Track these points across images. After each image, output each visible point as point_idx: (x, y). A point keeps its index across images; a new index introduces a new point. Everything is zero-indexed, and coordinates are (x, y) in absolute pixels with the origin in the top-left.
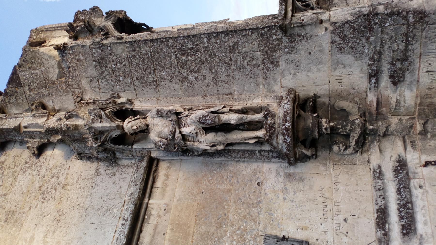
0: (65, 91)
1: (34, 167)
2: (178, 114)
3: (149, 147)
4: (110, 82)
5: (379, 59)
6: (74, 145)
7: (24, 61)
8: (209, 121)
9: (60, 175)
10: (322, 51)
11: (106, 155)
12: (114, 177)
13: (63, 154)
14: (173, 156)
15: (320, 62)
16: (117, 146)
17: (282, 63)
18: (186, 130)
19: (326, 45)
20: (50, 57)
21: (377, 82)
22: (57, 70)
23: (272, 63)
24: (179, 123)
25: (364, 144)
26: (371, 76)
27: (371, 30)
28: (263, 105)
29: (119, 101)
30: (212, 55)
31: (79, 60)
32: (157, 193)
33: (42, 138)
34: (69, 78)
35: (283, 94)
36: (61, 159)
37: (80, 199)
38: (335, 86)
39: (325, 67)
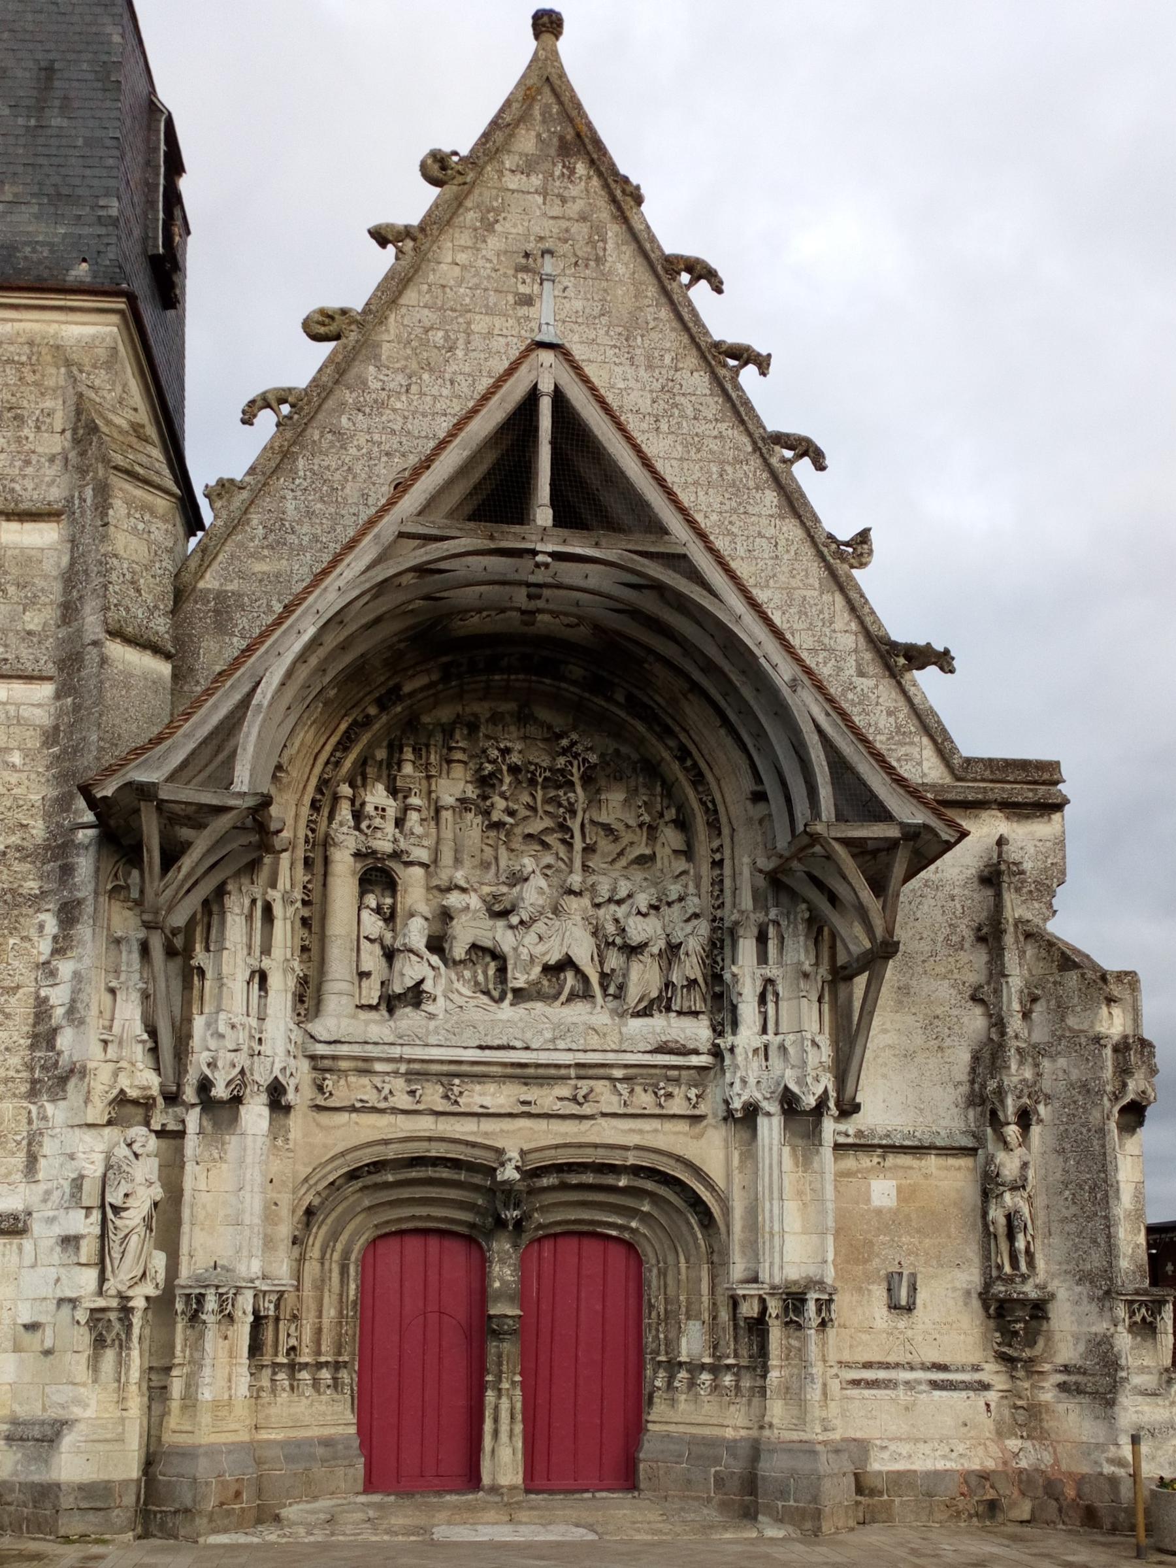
0: (1053, 1034)
2: (1024, 1187)
4: (1063, 1095)
5: (1079, 1373)
8: (1016, 1223)
10: (1089, 1325)
15: (1080, 1323)
17: (1079, 1289)
18: (1007, 1197)
19: (1094, 1329)
20: (1092, 1022)
21: (1061, 1371)
22: (1076, 1027)
23: (1080, 1279)
24: (1014, 1189)
25: (1003, 1359)
26: (1065, 1366)
27: (1105, 1366)
28: (1037, 1270)
29: (1041, 1108)
30: (1089, 1219)
31: (1087, 1059)
35: (1049, 1289)
38: (1057, 1336)
39: (1075, 1328)
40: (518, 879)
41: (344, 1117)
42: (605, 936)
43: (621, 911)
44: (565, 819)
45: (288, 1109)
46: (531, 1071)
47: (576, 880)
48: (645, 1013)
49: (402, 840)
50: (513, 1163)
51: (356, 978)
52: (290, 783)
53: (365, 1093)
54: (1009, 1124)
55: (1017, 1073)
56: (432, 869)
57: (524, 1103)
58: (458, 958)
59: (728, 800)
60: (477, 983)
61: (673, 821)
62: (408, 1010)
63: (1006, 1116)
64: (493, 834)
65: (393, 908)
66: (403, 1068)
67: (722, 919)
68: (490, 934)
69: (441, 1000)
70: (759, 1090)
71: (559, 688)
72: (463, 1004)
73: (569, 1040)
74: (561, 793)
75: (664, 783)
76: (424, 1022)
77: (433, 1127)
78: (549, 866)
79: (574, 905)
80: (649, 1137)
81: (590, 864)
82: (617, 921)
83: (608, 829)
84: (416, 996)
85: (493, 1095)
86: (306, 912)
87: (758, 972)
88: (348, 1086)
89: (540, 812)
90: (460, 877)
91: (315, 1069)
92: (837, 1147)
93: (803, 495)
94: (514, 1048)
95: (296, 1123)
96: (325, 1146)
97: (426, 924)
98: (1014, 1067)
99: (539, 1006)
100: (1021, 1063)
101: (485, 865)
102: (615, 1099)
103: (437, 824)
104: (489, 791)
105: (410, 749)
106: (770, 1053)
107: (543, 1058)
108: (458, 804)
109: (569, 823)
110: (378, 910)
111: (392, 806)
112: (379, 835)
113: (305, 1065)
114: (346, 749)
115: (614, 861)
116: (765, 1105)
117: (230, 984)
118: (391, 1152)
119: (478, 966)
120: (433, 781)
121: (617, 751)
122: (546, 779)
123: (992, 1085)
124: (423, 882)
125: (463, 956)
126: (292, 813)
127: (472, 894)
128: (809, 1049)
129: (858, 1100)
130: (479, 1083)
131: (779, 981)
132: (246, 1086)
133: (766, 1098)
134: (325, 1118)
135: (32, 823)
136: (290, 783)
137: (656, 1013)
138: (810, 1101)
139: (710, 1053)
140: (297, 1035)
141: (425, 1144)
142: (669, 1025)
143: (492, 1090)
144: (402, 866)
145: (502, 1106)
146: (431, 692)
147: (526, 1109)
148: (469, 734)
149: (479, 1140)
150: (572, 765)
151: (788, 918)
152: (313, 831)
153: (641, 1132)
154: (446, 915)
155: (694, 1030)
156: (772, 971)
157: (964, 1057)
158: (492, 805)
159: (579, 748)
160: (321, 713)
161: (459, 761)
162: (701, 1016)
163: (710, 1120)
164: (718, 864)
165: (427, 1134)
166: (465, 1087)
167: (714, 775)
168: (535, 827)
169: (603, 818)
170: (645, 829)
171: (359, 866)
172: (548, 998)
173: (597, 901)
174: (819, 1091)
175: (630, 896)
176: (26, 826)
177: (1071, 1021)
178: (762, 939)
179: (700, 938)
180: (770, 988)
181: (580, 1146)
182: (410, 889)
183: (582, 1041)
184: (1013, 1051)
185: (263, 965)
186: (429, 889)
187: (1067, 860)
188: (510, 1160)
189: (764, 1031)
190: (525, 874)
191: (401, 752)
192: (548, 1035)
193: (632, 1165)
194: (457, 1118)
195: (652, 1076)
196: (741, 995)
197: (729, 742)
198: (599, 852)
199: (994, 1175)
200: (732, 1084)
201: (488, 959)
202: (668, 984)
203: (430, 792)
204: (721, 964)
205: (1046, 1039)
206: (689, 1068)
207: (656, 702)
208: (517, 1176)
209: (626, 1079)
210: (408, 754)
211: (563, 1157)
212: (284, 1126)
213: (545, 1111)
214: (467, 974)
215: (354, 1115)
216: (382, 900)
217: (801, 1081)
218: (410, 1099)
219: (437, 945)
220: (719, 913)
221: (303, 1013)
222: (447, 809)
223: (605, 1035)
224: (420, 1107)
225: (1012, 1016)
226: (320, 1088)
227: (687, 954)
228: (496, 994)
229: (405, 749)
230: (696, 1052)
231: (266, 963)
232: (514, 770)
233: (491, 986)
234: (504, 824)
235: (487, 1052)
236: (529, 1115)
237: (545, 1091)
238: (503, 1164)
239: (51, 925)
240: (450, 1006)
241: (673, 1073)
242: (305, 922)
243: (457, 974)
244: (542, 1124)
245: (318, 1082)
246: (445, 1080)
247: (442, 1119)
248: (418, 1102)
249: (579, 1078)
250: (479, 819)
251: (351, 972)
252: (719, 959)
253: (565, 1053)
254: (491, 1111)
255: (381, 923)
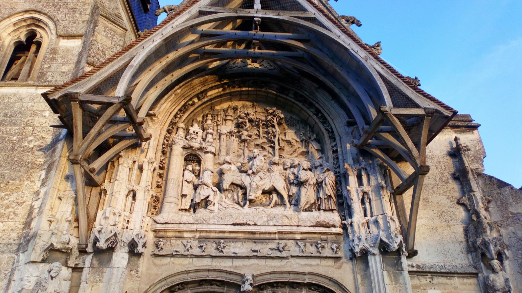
1: (452, 203)
3: (484, 272)
6: (472, 227)
7: (516, 191)
9: (453, 221)
11: (472, 247)
12: (460, 253)
13: (464, 218)
14: (482, 286)
16: (480, 255)
32: (461, 280)
33: (470, 206)
34: (512, 219)
36: (460, 218)
37: (445, 237)
40: (251, 159)
41: (167, 260)
42: (289, 180)
43: (295, 170)
44: (271, 138)
45: (139, 255)
46: (257, 236)
47: (276, 159)
48: (309, 210)
49: (204, 143)
50: (249, 282)
51: (180, 197)
52: (158, 122)
53: (179, 248)
54: (493, 259)
55: (491, 235)
56: (217, 156)
57: (254, 251)
58: (225, 188)
59: (337, 127)
60: (234, 199)
61: (315, 139)
62: (202, 210)
63: (491, 255)
64: (242, 145)
65: (199, 171)
66: (197, 235)
67: (339, 172)
68: (239, 178)
69: (217, 205)
70: (367, 243)
71: (268, 93)
72: (227, 206)
73: (275, 221)
74: (270, 129)
75: (310, 127)
76: (209, 214)
77: (210, 264)
78: (265, 156)
79: (275, 168)
80: (315, 268)
81: (282, 155)
82: (294, 174)
83: (289, 142)
84: (206, 202)
85: (240, 248)
86: (161, 172)
87: (359, 189)
88: (171, 244)
89: (261, 136)
90: (228, 159)
91: (156, 237)
92: (410, 272)
93: (354, 33)
94: (249, 225)
95: (144, 263)
96: (157, 275)
97: (212, 174)
98: (488, 232)
99: (261, 208)
100: (491, 230)
101: (239, 156)
102: (297, 249)
103: (220, 141)
104: (241, 129)
105: (211, 116)
106: (370, 225)
107: (263, 229)
108: (228, 134)
109: (273, 139)
110: (193, 172)
111: (200, 131)
112: (194, 140)
113: (151, 236)
114: (184, 113)
115: (291, 154)
116: (371, 249)
117: (117, 195)
118: (189, 278)
119: (234, 192)
120: (219, 127)
121: (291, 117)
122: (263, 124)
123: (479, 241)
124: (212, 160)
125: (227, 187)
126: (159, 133)
127: (233, 165)
128: (390, 221)
129: (415, 249)
130: (233, 242)
131: (370, 193)
132: (117, 243)
133: (371, 247)
134: (158, 261)
135: (47, 136)
136: (158, 122)
137: (314, 210)
138: (395, 246)
139: (340, 227)
140: (148, 221)
141: (206, 273)
142: (320, 214)
143: (239, 245)
144: (204, 154)
145: (244, 253)
146: (219, 94)
147: (255, 254)
148: (234, 112)
149: (232, 270)
150: (274, 119)
151: (370, 166)
152: (167, 141)
153: (311, 265)
154: (221, 173)
155: (332, 217)
156: (366, 187)
157: (459, 229)
158: (242, 134)
159: (276, 113)
160: (174, 98)
161: (229, 120)
162: (334, 211)
163: (344, 260)
164: (335, 152)
165: (207, 268)
166: (226, 244)
167: (331, 118)
168: (260, 141)
169: (287, 138)
170: (304, 142)
171: (185, 152)
172: (265, 205)
173: (285, 167)
174: (398, 242)
175: (299, 164)
176: (44, 138)
177: (511, 209)
178: (359, 178)
179: (331, 178)
180: (366, 196)
181: (282, 273)
182: (206, 162)
183: (281, 222)
184: (486, 225)
185: (134, 188)
186: (215, 164)
187: (485, 148)
188: (247, 280)
189: (365, 215)
190: (255, 156)
191: (207, 116)
192: (265, 219)
193: (308, 283)
194: (222, 259)
195: (314, 238)
196: (352, 199)
197: (336, 105)
198: (285, 150)
199: (492, 286)
200: (353, 240)
201: (239, 189)
202: (319, 198)
203: (217, 130)
204: (341, 190)
205: (500, 219)
206: (331, 234)
207: (305, 94)
208: (251, 288)
209: (302, 240)
210: (210, 117)
211: (274, 279)
212: (137, 264)
213: (264, 255)
214: (230, 196)
215: (172, 259)
216: (194, 168)
217: (389, 236)
218: (200, 250)
219: (219, 186)
220: (338, 170)
221: (155, 213)
222: (224, 134)
223: (291, 219)
224: (204, 254)
225: (481, 209)
226: (157, 246)
227: (326, 185)
228: (242, 204)
229: (208, 116)
230: (334, 226)
231: (136, 188)
232: (251, 121)
233: (240, 200)
234: (247, 140)
235: (237, 227)
236: (257, 257)
237: (264, 245)
238: (244, 283)
239: (43, 176)
240: (221, 207)
241: (324, 237)
242: (160, 176)
243: (225, 196)
244: (263, 262)
245: (156, 243)
246: (217, 241)
247: (215, 260)
248: (203, 251)
249: (280, 239)
250: (237, 139)
251: (178, 194)
252: (340, 188)
253: (273, 227)
254: (238, 255)
255: (195, 177)
